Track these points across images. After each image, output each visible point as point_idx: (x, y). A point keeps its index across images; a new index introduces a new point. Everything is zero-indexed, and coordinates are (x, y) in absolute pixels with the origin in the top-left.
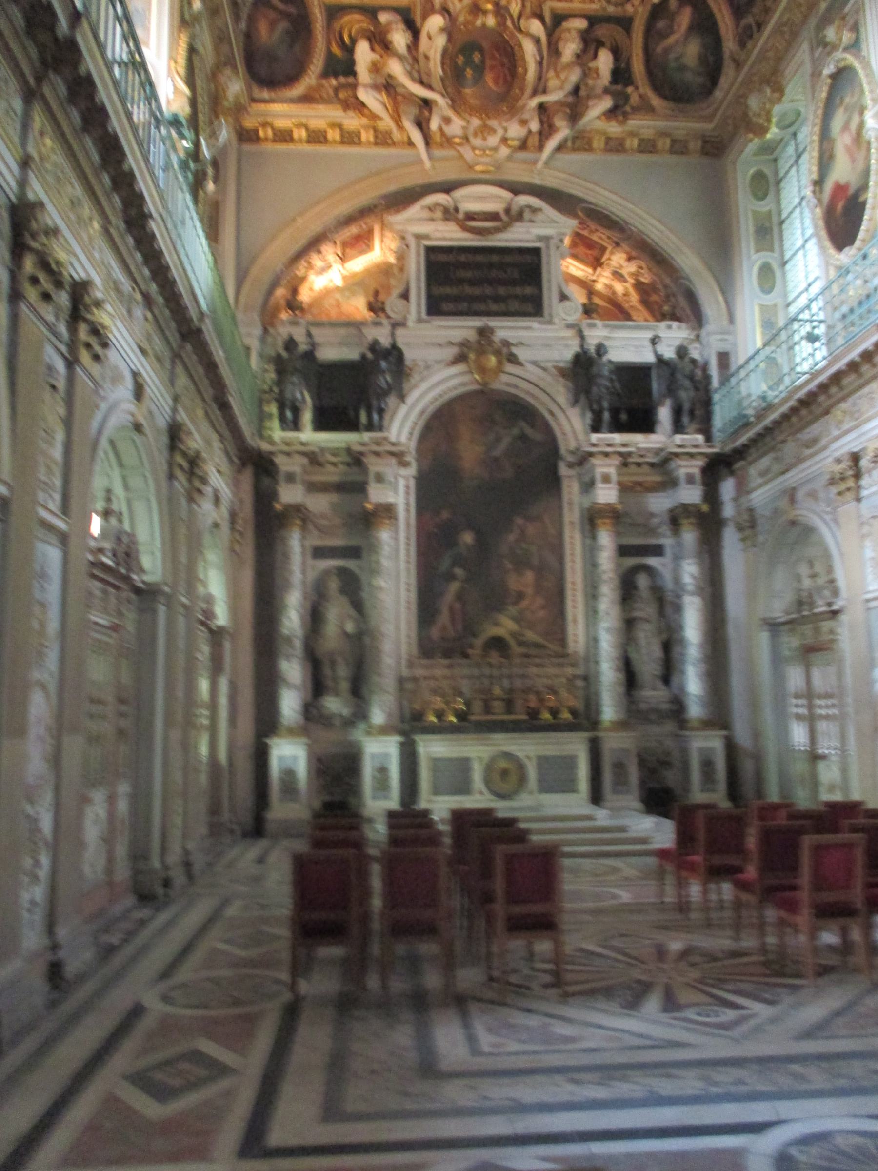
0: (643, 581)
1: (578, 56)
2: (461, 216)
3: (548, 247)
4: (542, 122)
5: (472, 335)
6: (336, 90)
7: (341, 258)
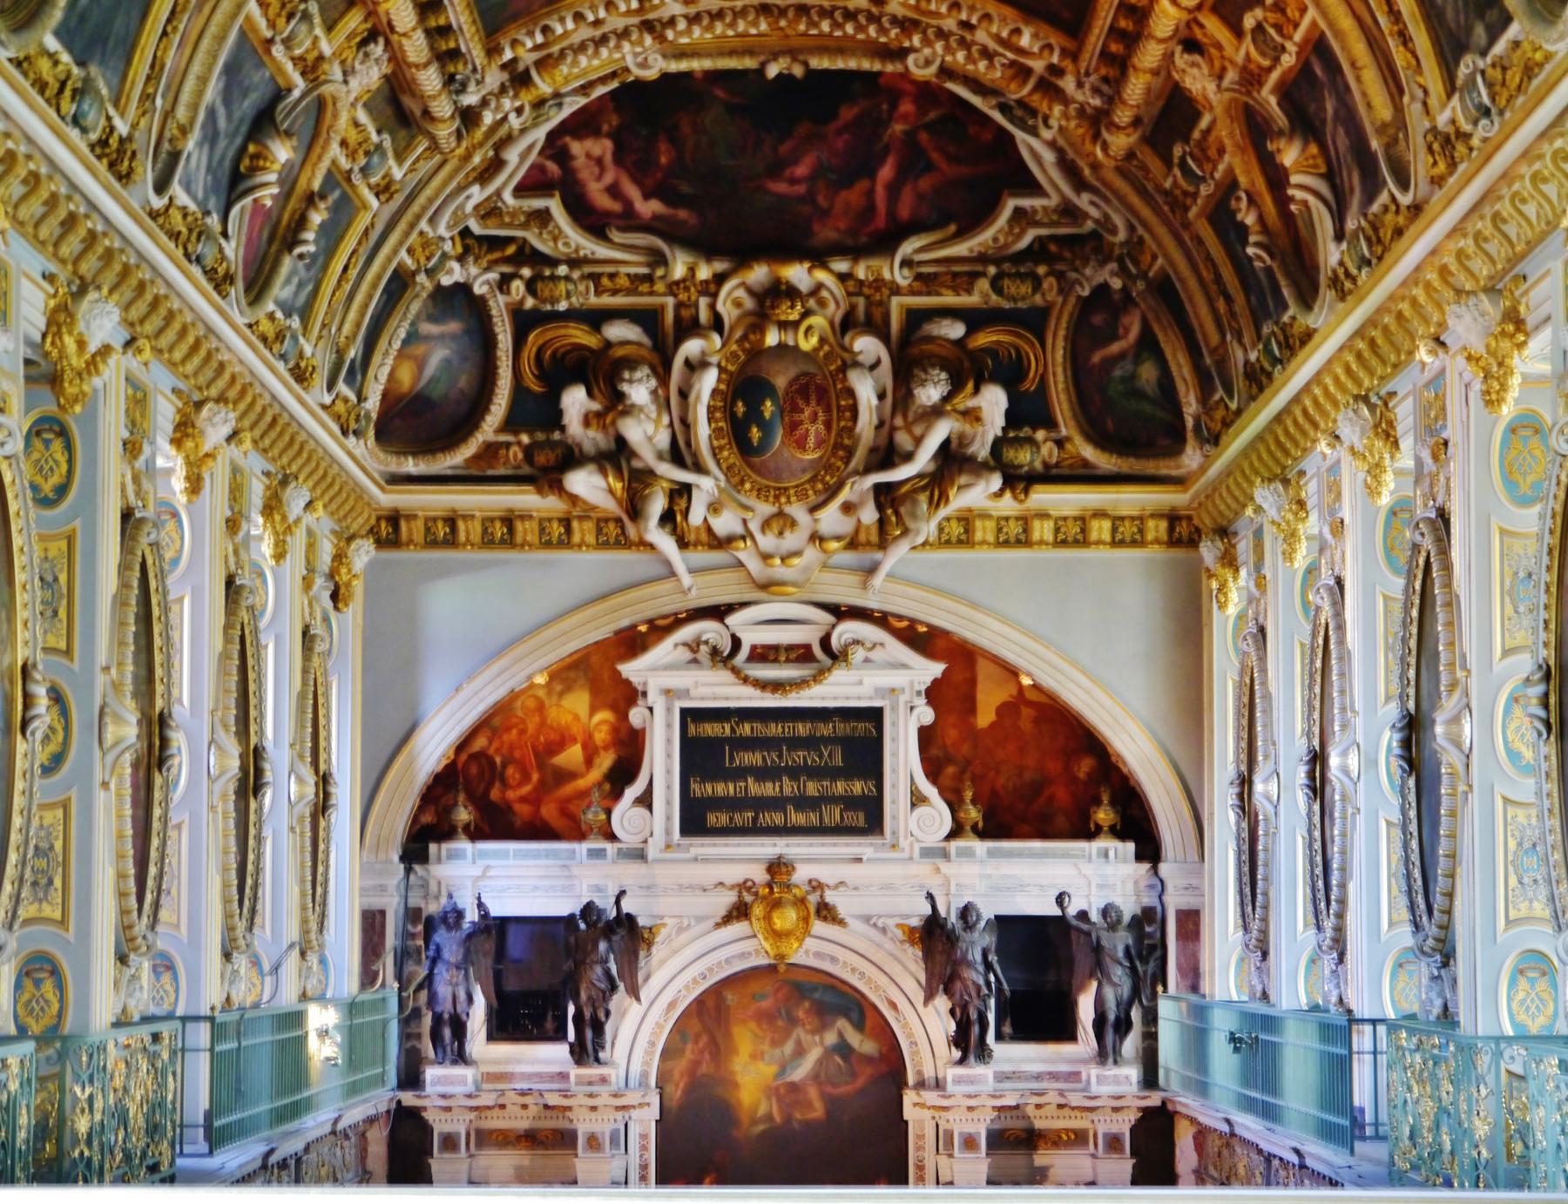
1: (946, 399)
2: (744, 652)
3: (894, 709)
4: (880, 507)
5: (759, 875)
6: (529, 452)
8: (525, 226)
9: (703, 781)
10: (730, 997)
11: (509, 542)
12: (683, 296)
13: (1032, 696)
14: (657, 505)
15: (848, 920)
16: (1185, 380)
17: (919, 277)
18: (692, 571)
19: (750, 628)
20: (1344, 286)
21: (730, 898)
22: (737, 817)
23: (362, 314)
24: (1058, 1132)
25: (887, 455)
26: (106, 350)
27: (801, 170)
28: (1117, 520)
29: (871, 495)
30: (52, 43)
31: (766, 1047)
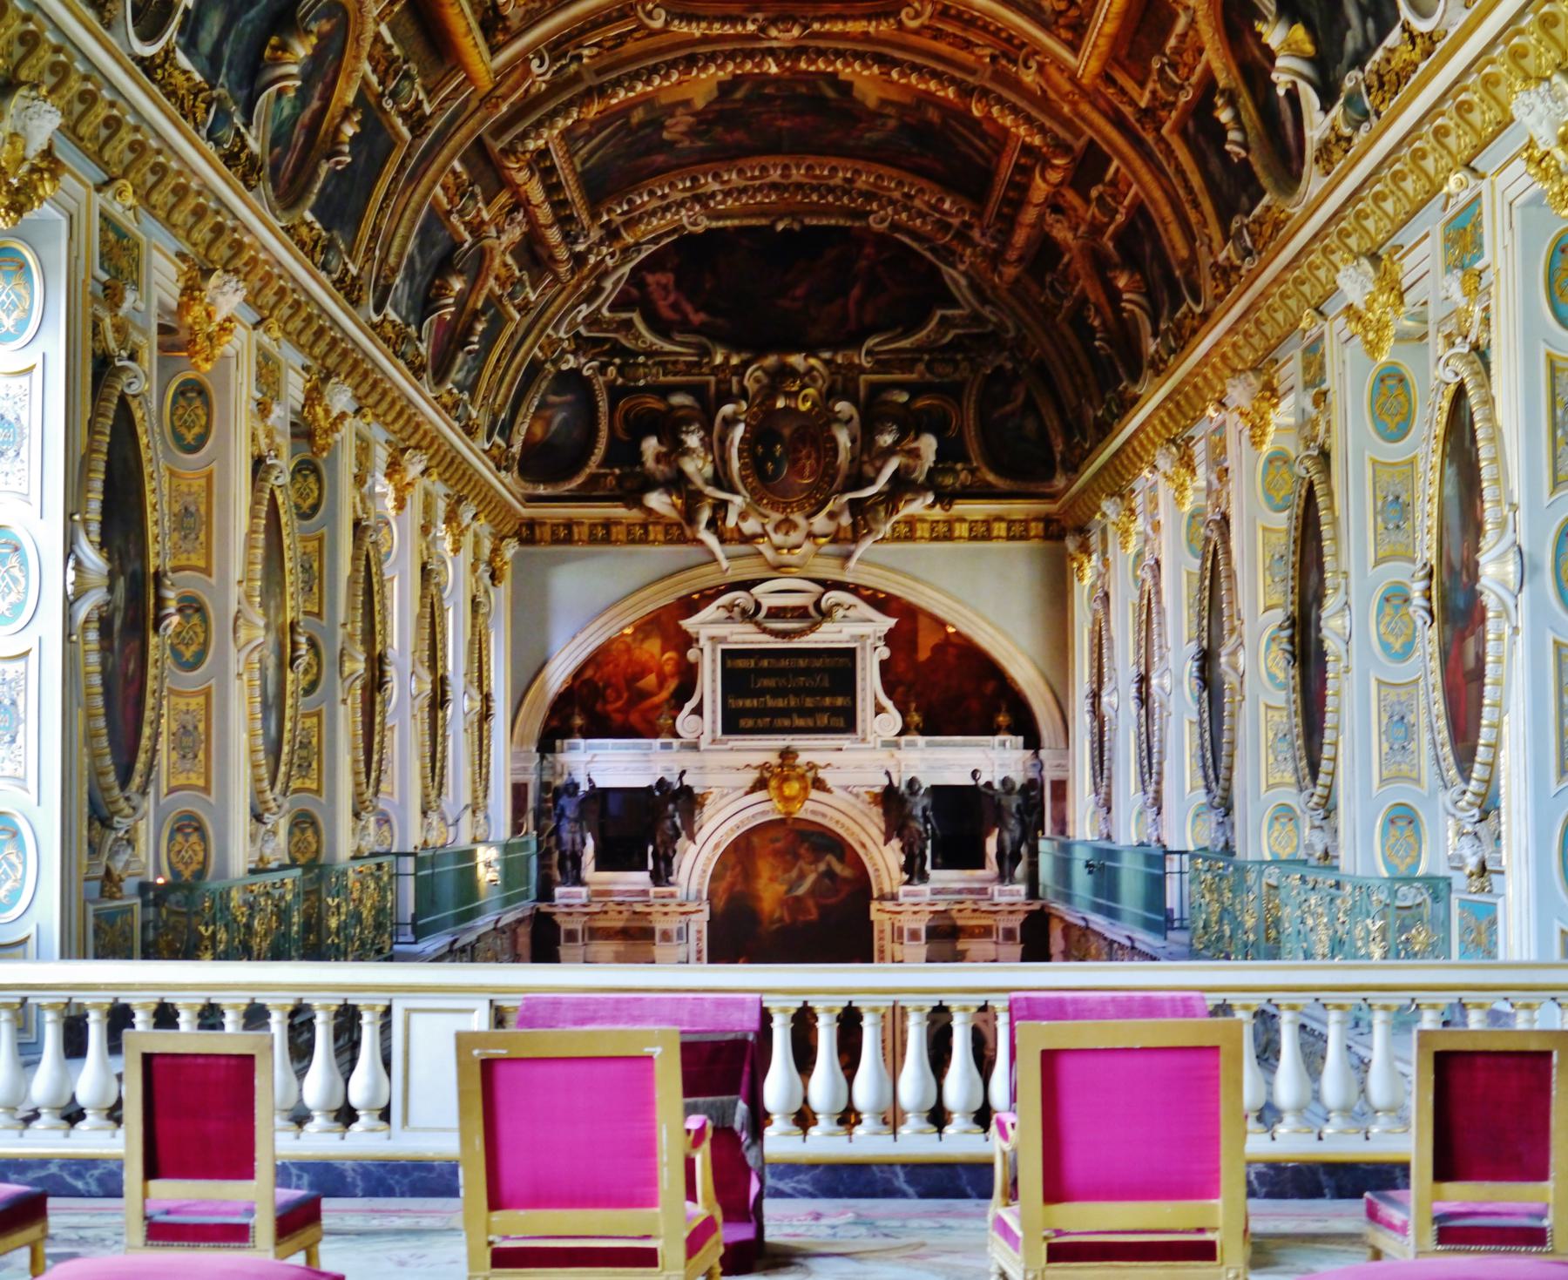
3: (863, 648)
4: (853, 515)
5: (774, 759)
6: (619, 479)
8: (616, 331)
9: (737, 697)
10: (755, 840)
11: (607, 540)
12: (721, 376)
13: (954, 640)
14: (705, 515)
17: (877, 362)
18: (728, 558)
19: (766, 594)
20: (1159, 368)
21: (755, 775)
23: (509, 390)
26: (342, 416)
27: (799, 292)
28: (1011, 523)
30: (309, 217)
31: (779, 873)
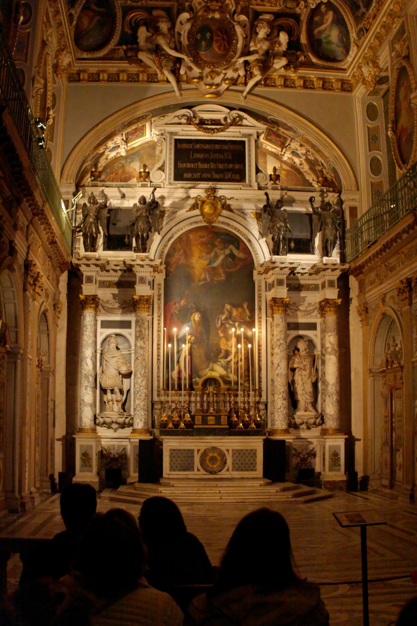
0: (301, 345)
1: (268, 35)
2: (197, 122)
3: (249, 141)
4: (246, 71)
6: (125, 52)
7: (125, 142)
9: (182, 163)
10: (191, 236)
15: (234, 210)
16: (351, 24)
22: (195, 174)
24: (309, 285)
25: (249, 53)
29: (243, 65)
31: (204, 254)
